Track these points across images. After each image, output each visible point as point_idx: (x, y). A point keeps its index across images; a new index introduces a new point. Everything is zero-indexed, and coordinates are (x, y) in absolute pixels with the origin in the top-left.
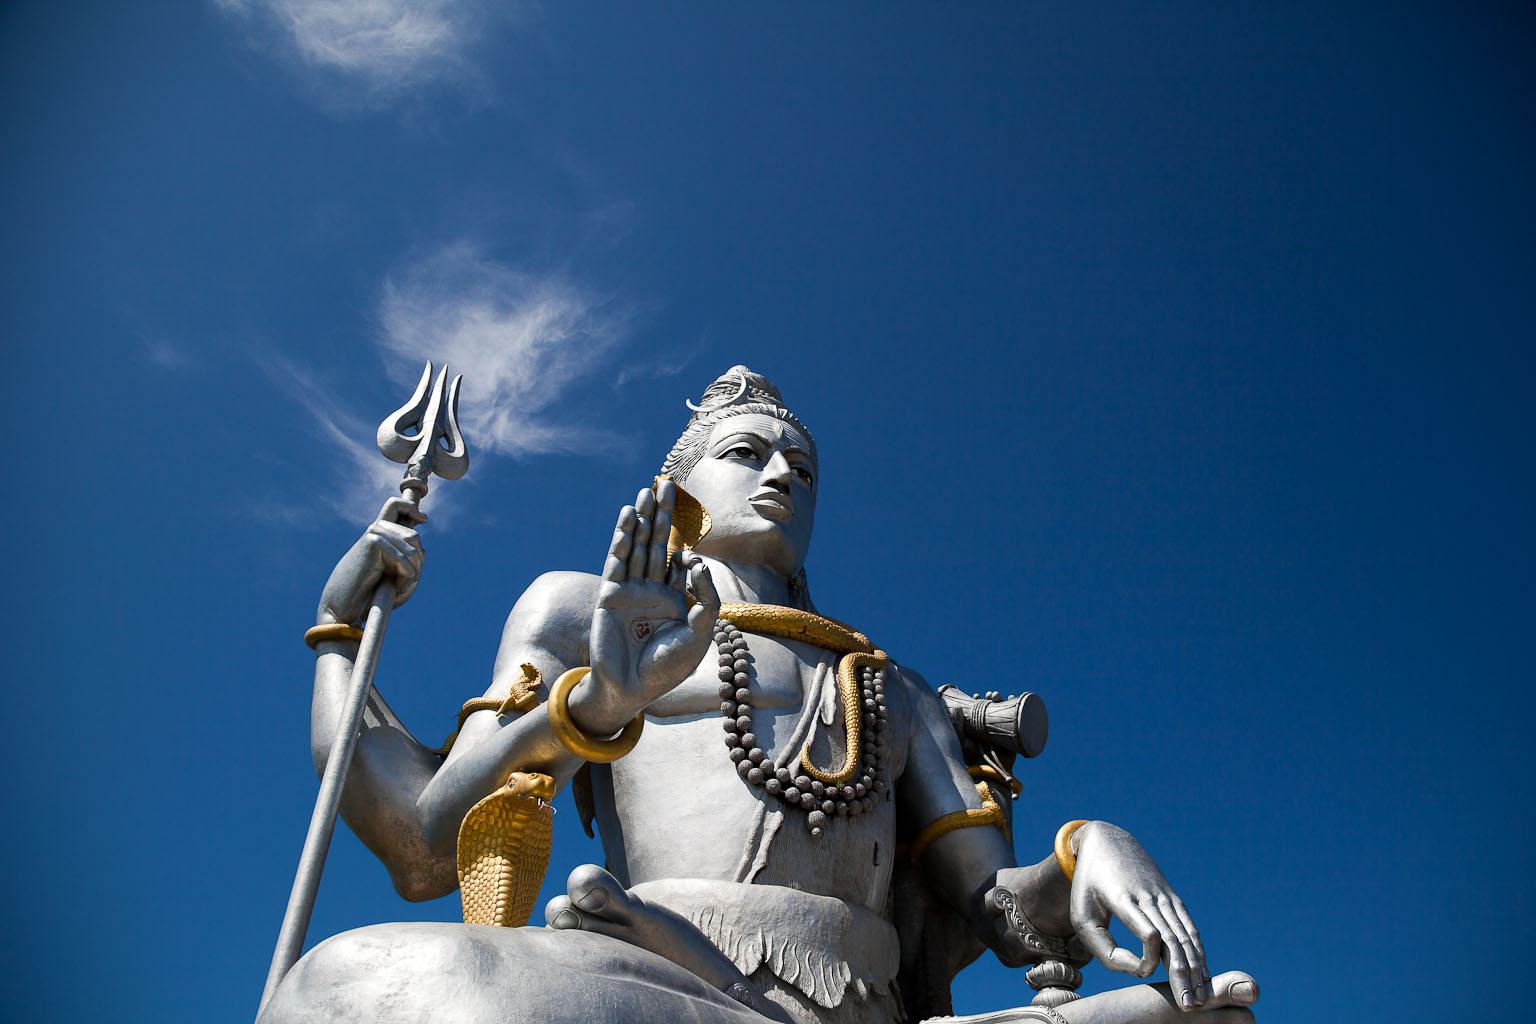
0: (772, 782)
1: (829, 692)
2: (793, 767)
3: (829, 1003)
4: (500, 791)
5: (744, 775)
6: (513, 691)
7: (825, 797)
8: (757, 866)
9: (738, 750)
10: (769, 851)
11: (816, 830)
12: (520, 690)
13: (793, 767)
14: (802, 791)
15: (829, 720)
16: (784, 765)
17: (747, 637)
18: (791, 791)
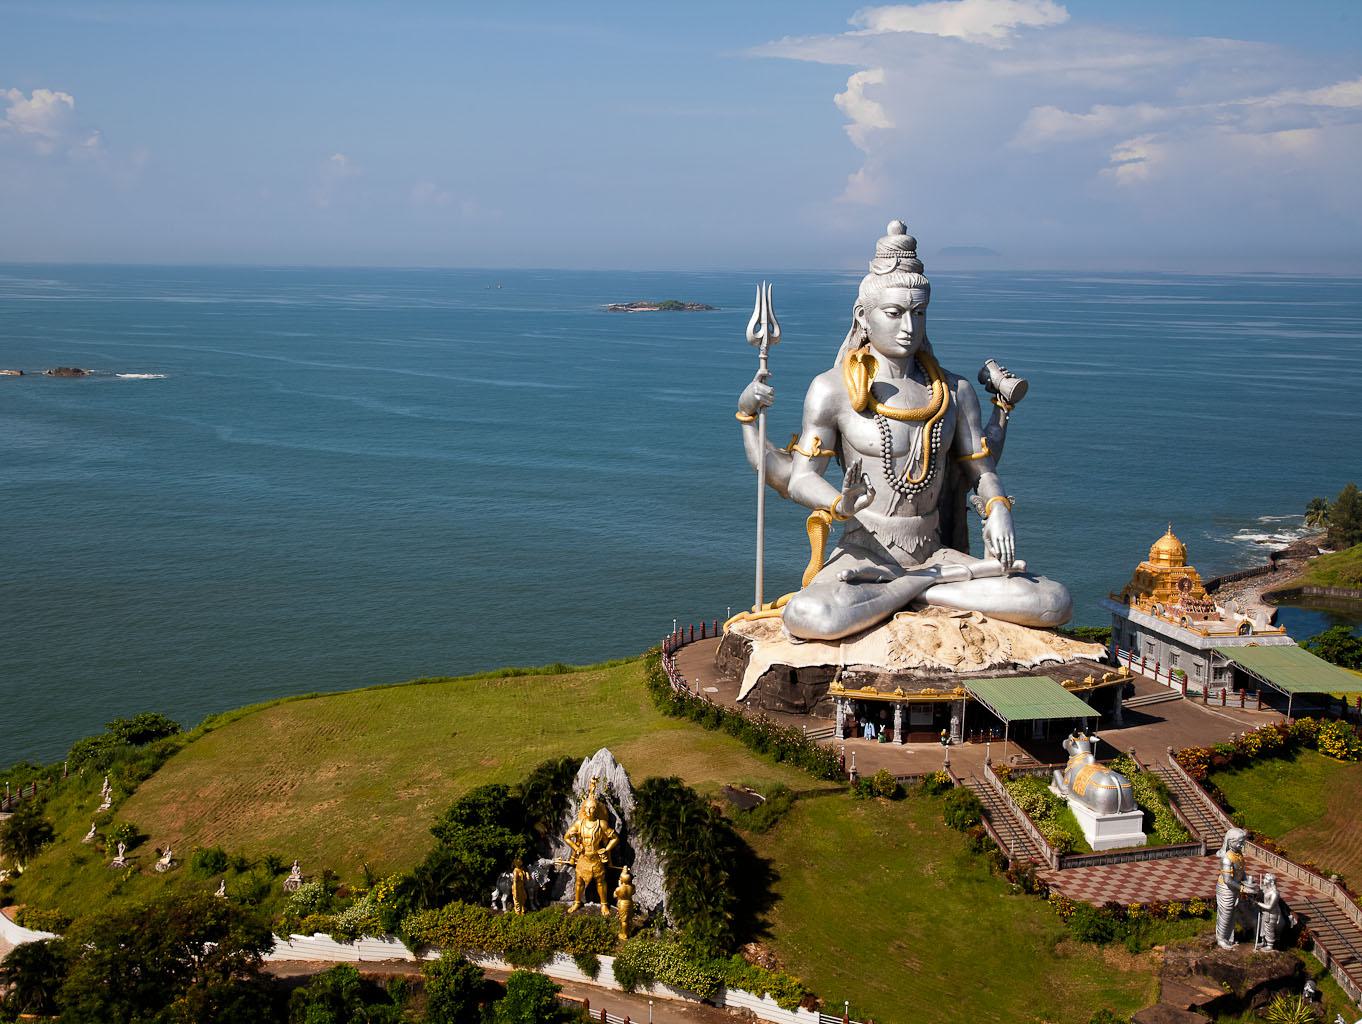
1: (919, 444)
2: (904, 479)
7: (913, 489)
8: (892, 510)
12: (814, 449)
13: (904, 479)
18: (902, 490)
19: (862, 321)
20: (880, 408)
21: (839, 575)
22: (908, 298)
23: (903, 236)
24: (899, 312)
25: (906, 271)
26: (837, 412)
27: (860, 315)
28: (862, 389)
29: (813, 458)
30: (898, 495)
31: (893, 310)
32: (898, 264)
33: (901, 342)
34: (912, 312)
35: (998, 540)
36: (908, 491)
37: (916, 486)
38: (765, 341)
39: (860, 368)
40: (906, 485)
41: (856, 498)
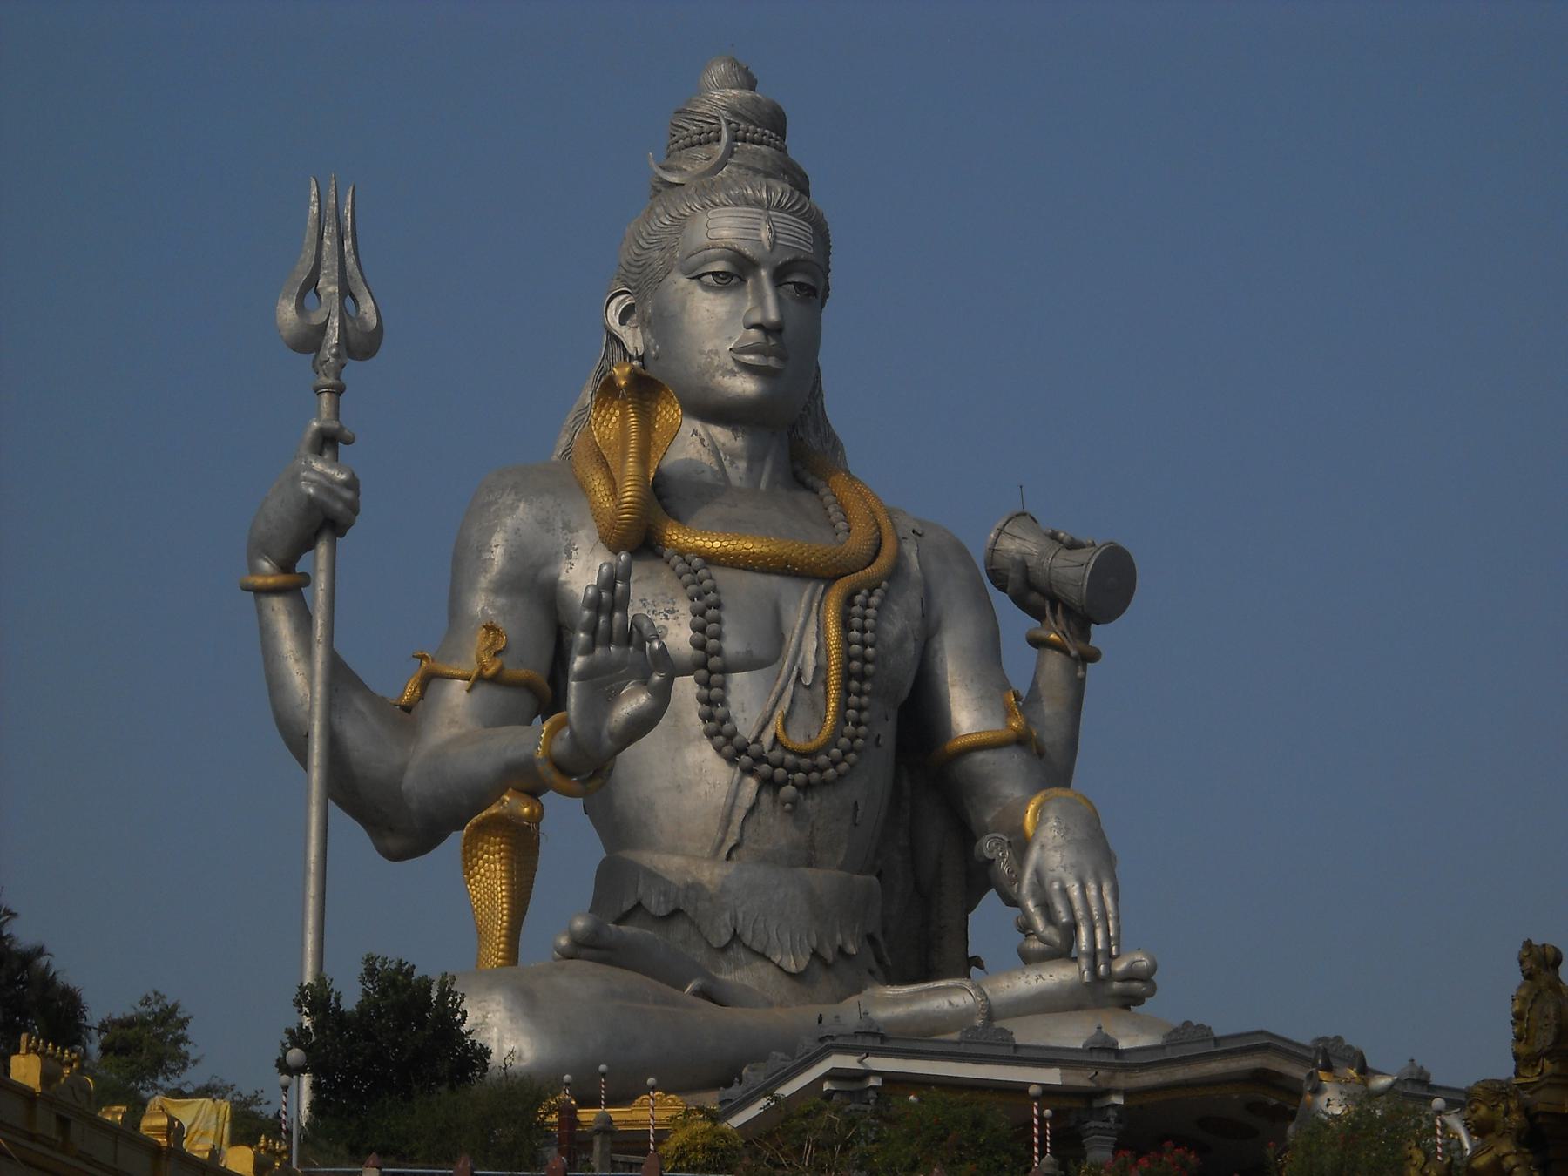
0: (745, 759)
1: (811, 645)
2: (767, 739)
3: (793, 969)
4: (494, 810)
5: (718, 750)
6: (479, 660)
7: (797, 769)
9: (712, 725)
10: (742, 828)
11: (788, 806)
14: (774, 767)
15: (808, 679)
16: (757, 740)
17: (723, 576)
18: (764, 768)
19: (633, 339)
20: (676, 536)
21: (563, 941)
22: (765, 235)
23: (748, 94)
24: (736, 272)
25: (756, 171)
26: (551, 559)
27: (622, 322)
28: (631, 467)
29: (479, 680)
30: (751, 783)
31: (719, 267)
32: (730, 152)
33: (749, 358)
34: (780, 276)
35: (1064, 891)
36: (780, 772)
37: (806, 762)
38: (333, 337)
39: (624, 418)
40: (777, 753)
41: (612, 698)
